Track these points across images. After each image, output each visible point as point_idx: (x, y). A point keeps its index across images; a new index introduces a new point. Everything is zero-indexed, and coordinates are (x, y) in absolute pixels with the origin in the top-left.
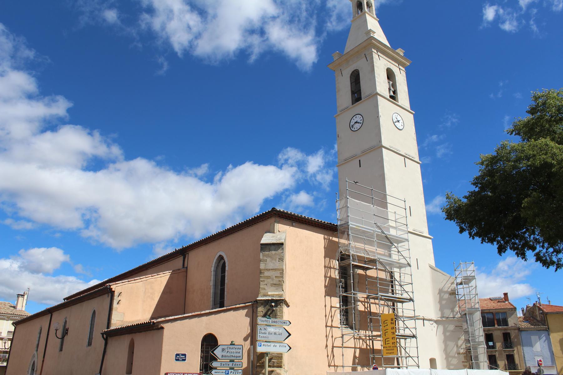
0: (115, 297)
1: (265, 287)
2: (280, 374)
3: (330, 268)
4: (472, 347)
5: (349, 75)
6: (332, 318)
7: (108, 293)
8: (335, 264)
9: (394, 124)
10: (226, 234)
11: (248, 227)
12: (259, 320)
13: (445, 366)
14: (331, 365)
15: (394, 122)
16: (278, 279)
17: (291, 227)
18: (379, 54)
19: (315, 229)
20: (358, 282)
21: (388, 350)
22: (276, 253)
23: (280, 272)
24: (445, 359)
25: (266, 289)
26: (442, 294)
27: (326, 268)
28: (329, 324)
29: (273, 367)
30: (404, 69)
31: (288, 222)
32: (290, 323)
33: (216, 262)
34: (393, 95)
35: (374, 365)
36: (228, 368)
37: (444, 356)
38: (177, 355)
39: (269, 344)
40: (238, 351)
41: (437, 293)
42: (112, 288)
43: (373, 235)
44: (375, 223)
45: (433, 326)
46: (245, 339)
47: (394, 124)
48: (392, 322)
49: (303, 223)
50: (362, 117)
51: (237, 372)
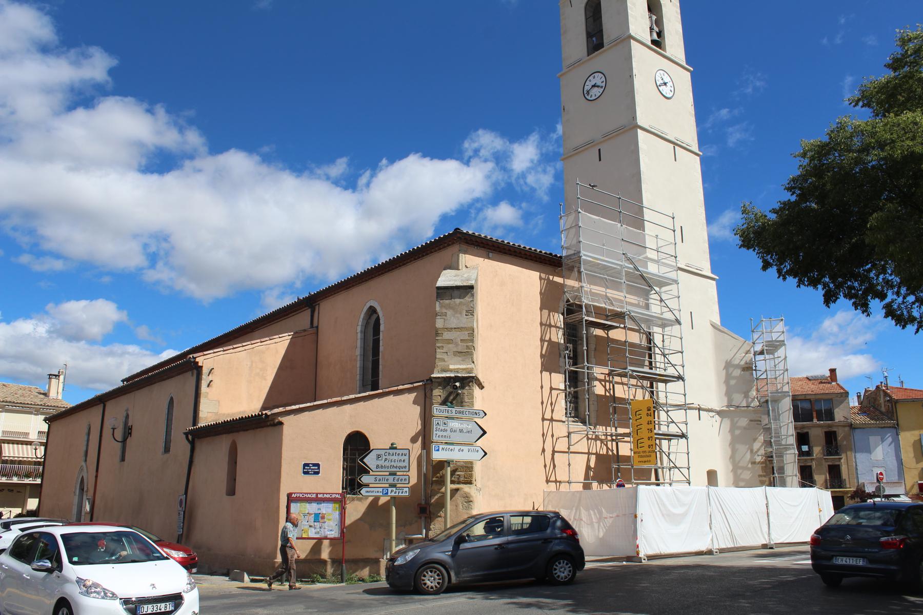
0: (203, 376)
1: (445, 356)
2: (469, 493)
3: (550, 326)
4: (775, 454)
6: (553, 406)
7: (191, 369)
8: (558, 319)
10: (380, 273)
11: (415, 259)
12: (435, 410)
14: (550, 480)
15: (658, 84)
16: (466, 344)
17: (486, 260)
19: (526, 263)
20: (595, 349)
21: (642, 457)
22: (461, 302)
23: (469, 332)
24: (732, 471)
25: (446, 360)
26: (731, 369)
27: (543, 327)
28: (548, 416)
29: (459, 483)
31: (482, 251)
32: (486, 414)
33: (364, 317)
35: (619, 479)
36: (388, 485)
37: (731, 468)
38: (305, 465)
39: (451, 447)
40: (403, 458)
41: (723, 368)
42: (198, 362)
43: (619, 272)
44: (623, 254)
45: (714, 419)
46: (414, 440)
47: (658, 88)
48: (649, 412)
49: (505, 253)
50: (603, 77)
51: (401, 491)
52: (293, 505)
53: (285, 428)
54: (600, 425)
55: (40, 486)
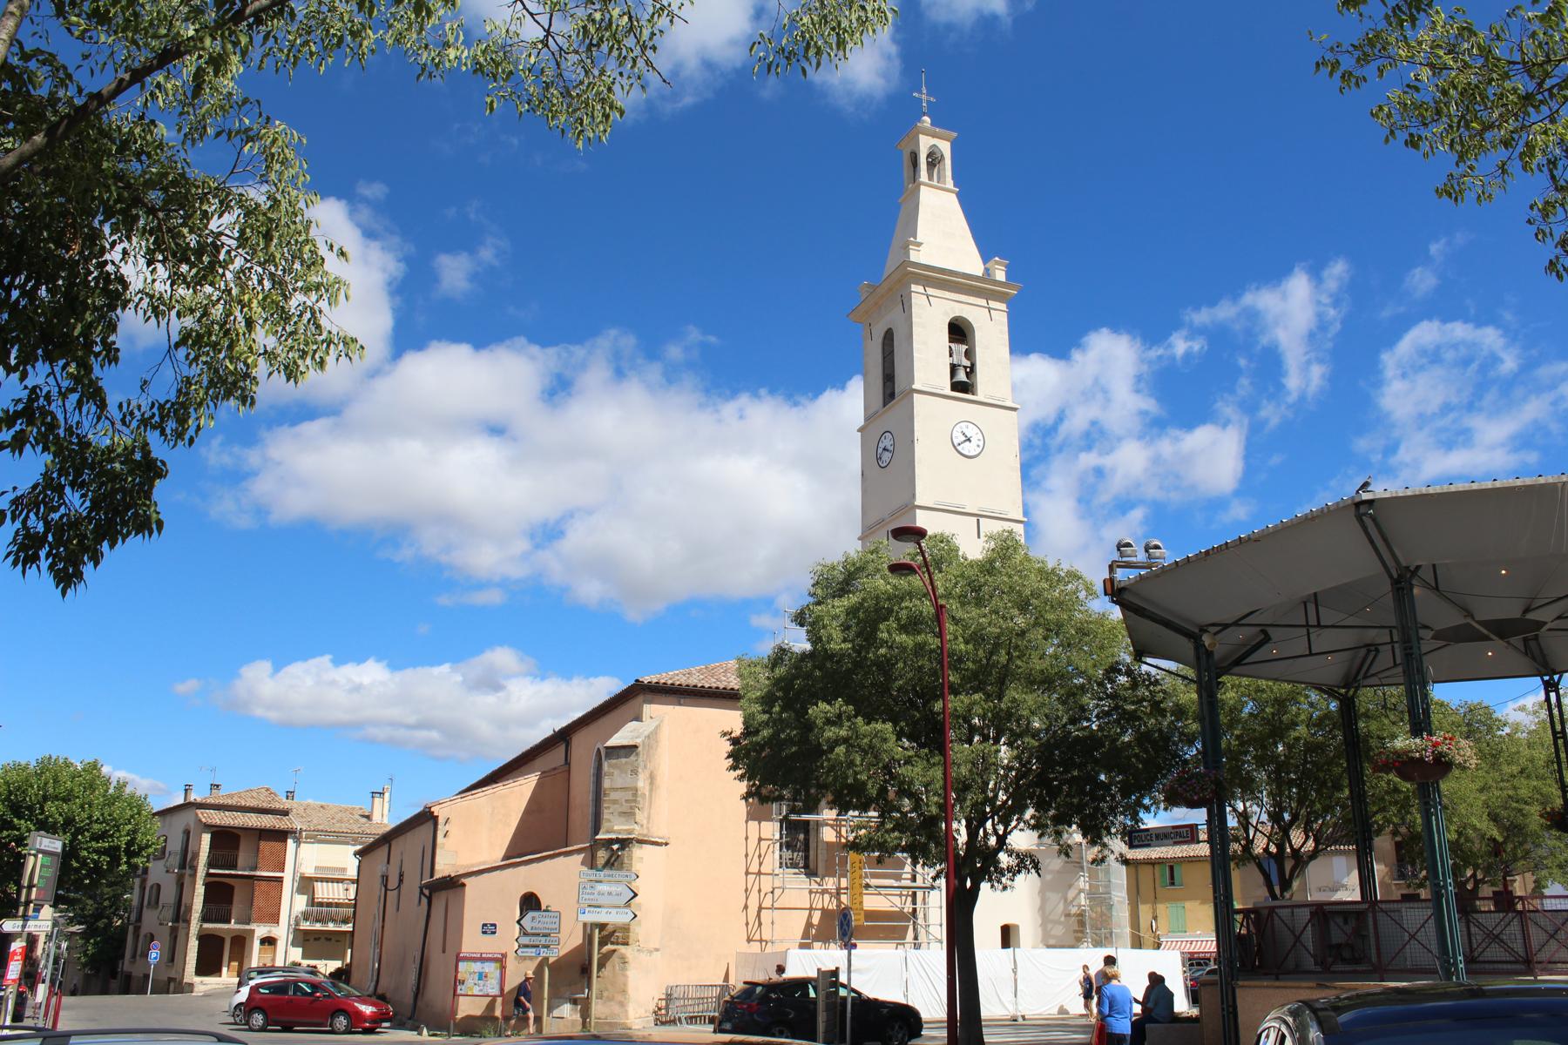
1: (611, 817)
5: (880, 340)
9: (957, 450)
13: (1040, 939)
18: (930, 291)
28: (754, 868)
29: (618, 944)
30: (1003, 306)
31: (671, 698)
34: (965, 379)
38: (484, 925)
47: (957, 450)
52: (460, 964)
53: (467, 889)
54: (829, 876)
55: (352, 933)
